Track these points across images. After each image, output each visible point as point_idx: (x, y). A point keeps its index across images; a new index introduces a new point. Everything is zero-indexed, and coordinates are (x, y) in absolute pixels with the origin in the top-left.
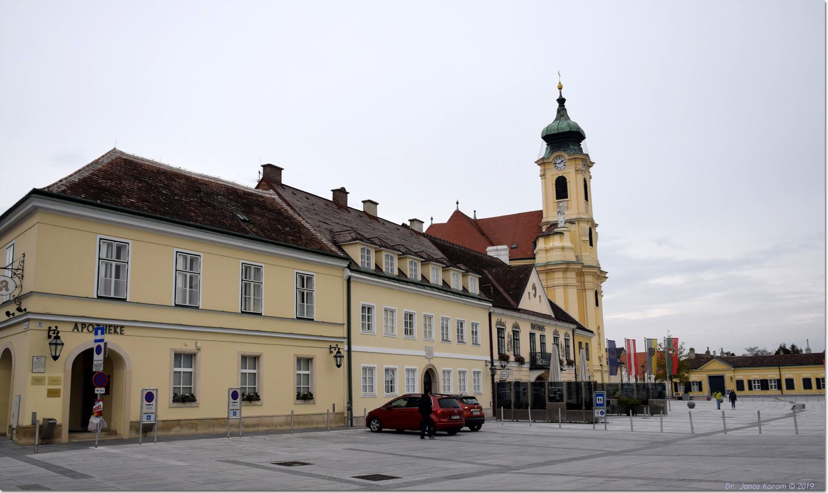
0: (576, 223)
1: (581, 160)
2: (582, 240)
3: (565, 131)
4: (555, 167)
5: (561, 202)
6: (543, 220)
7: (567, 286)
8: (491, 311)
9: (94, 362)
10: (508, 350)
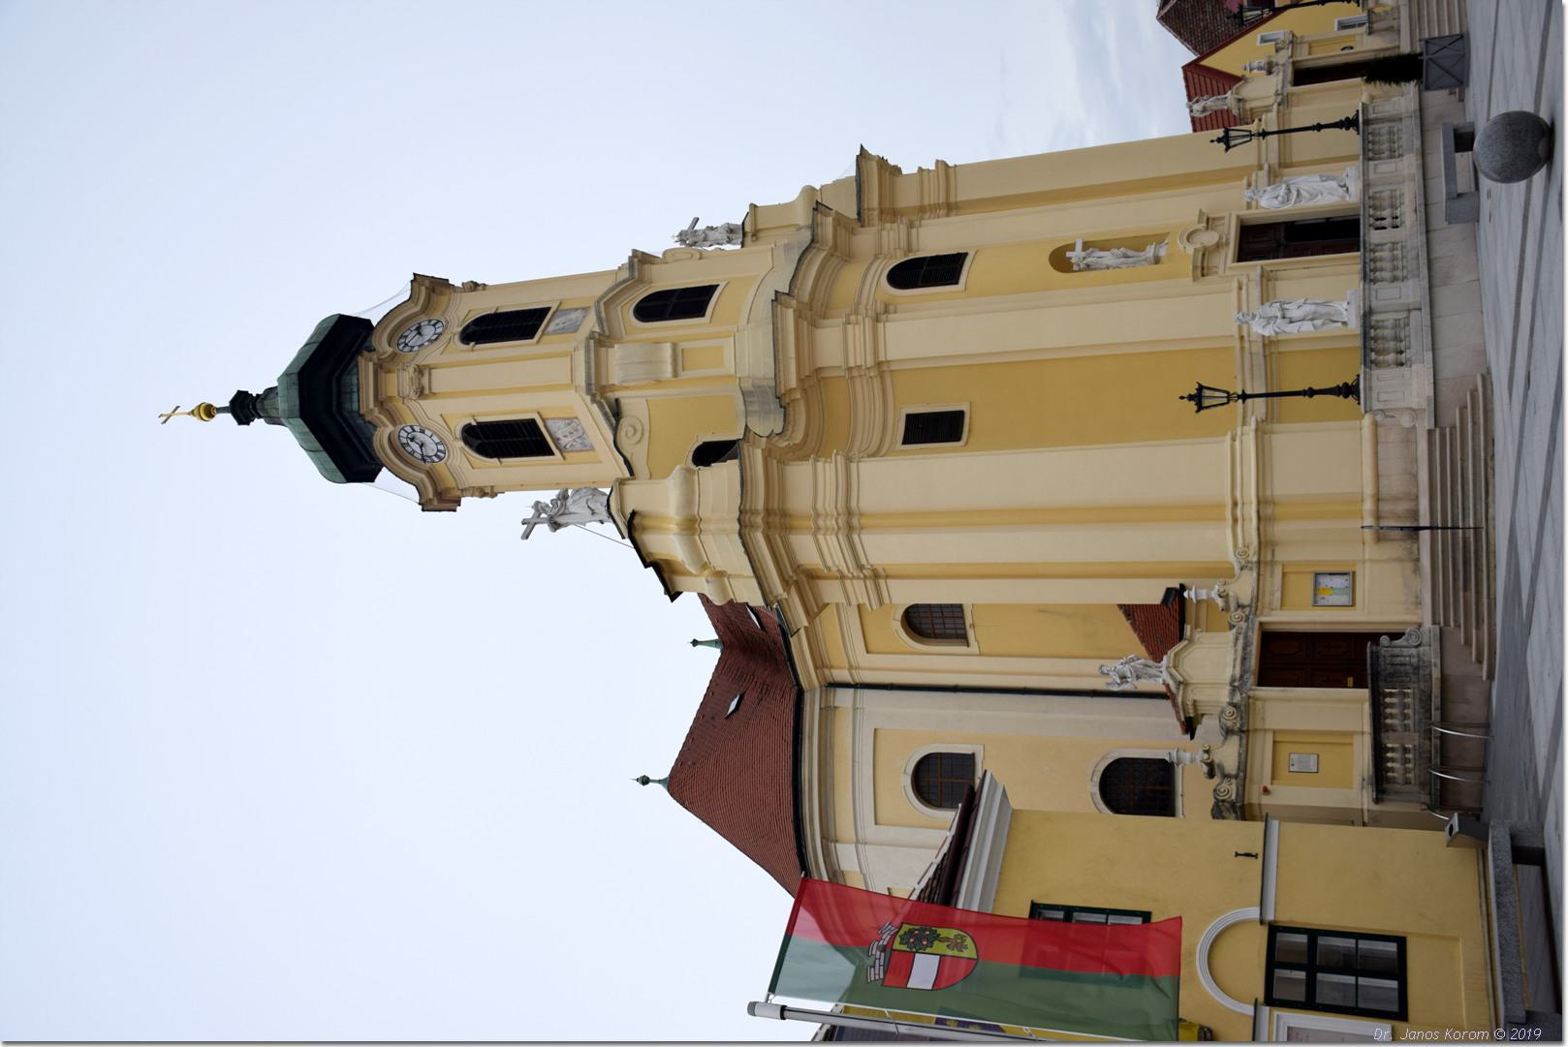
0: (612, 396)
1: (382, 375)
2: (675, 374)
4: (441, 459)
5: (556, 441)
7: (850, 513)
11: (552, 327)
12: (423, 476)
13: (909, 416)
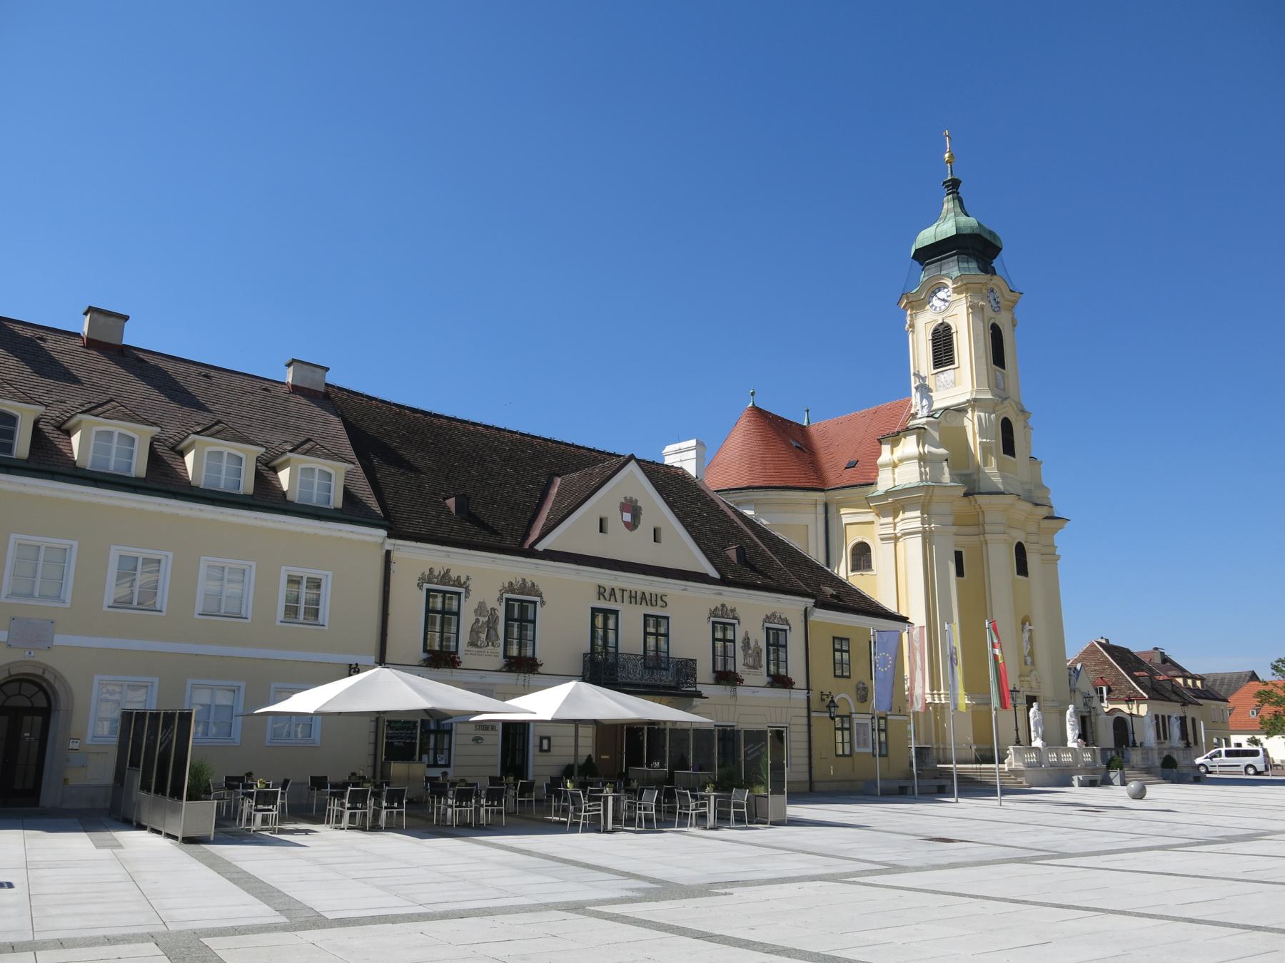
3: (949, 236)
8: (387, 547)
10: (473, 644)
11: (998, 373)
12: (922, 297)
13: (961, 552)
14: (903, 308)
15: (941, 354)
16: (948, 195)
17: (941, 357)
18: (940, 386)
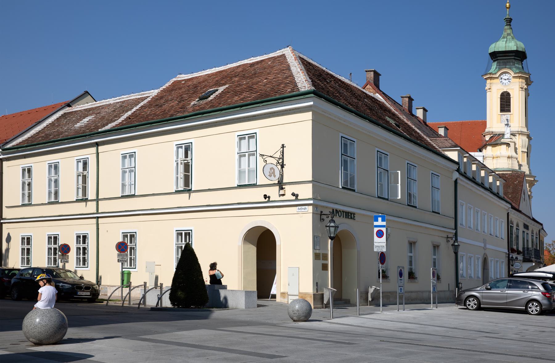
6: (487, 130)
9: (375, 244)
14: (485, 79)
15: (504, 106)
16: (506, 25)
17: (504, 108)
18: (502, 121)
